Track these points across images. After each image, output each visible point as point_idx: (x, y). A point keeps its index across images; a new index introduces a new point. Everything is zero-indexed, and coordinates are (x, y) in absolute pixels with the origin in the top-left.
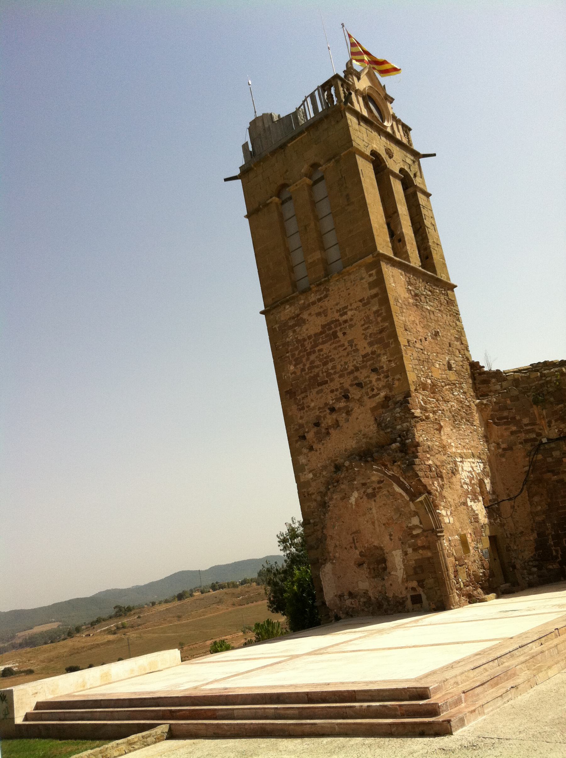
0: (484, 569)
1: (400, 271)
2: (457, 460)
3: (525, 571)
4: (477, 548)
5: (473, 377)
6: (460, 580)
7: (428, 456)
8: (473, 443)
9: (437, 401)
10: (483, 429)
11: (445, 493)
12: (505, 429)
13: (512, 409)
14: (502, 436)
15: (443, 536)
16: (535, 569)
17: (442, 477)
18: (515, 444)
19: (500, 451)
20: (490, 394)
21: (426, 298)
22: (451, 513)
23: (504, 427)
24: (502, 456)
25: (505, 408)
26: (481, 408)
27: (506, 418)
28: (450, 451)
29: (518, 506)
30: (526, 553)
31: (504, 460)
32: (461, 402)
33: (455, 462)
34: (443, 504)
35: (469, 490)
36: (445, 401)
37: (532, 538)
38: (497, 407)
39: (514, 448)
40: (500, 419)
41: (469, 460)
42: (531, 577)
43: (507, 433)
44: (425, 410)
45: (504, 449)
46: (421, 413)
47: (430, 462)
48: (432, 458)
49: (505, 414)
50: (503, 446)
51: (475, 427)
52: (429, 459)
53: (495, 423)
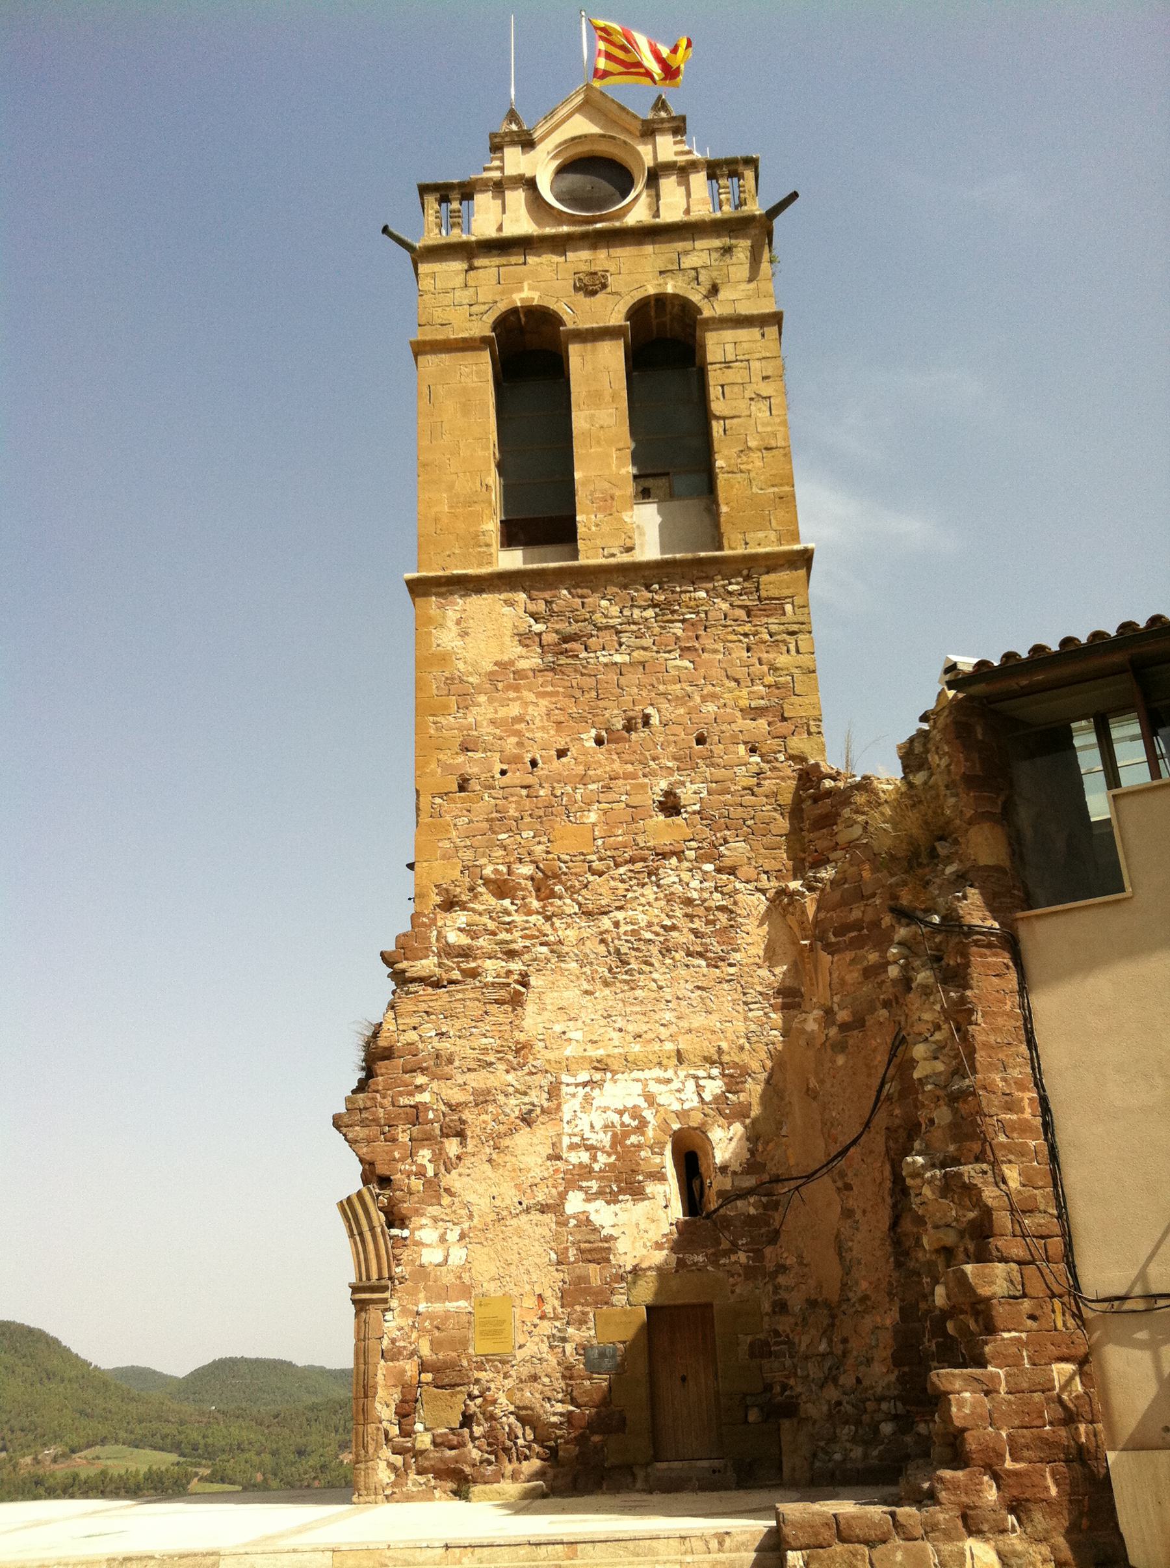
0: (573, 1401)
1: (504, 596)
2: (565, 1078)
3: (846, 1431)
4: (564, 1340)
5: (796, 812)
6: (419, 1427)
7: (421, 1080)
8: (699, 1021)
9: (548, 918)
10: (780, 970)
11: (452, 1180)
12: (853, 961)
13: (874, 895)
14: (843, 982)
15: (385, 1301)
16: (887, 1428)
17: (461, 1135)
18: (872, 1010)
19: (833, 1032)
20: (832, 856)
21: (618, 632)
22: (462, 1236)
23: (849, 955)
24: (840, 1047)
25: (860, 895)
26: (782, 903)
27: (857, 925)
28: (550, 1055)
29: (864, 1212)
30: (878, 1368)
31: (841, 1060)
32: (689, 902)
33: (554, 1091)
34: (433, 1210)
35: (596, 1167)
36: (588, 914)
37: (888, 1322)
38: (837, 895)
39: (870, 1021)
40: (840, 931)
41: (636, 1074)
42: (857, 1452)
43: (853, 976)
44: (466, 956)
45: (844, 1027)
46: (440, 965)
47: (425, 1097)
48: (434, 1085)
49: (856, 914)
50: (843, 1016)
51: (732, 970)
52: (420, 1088)
53: (830, 949)
